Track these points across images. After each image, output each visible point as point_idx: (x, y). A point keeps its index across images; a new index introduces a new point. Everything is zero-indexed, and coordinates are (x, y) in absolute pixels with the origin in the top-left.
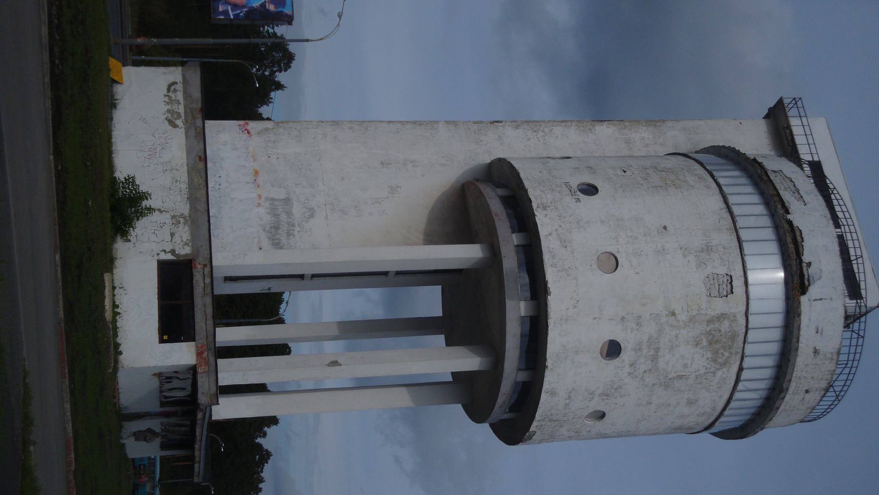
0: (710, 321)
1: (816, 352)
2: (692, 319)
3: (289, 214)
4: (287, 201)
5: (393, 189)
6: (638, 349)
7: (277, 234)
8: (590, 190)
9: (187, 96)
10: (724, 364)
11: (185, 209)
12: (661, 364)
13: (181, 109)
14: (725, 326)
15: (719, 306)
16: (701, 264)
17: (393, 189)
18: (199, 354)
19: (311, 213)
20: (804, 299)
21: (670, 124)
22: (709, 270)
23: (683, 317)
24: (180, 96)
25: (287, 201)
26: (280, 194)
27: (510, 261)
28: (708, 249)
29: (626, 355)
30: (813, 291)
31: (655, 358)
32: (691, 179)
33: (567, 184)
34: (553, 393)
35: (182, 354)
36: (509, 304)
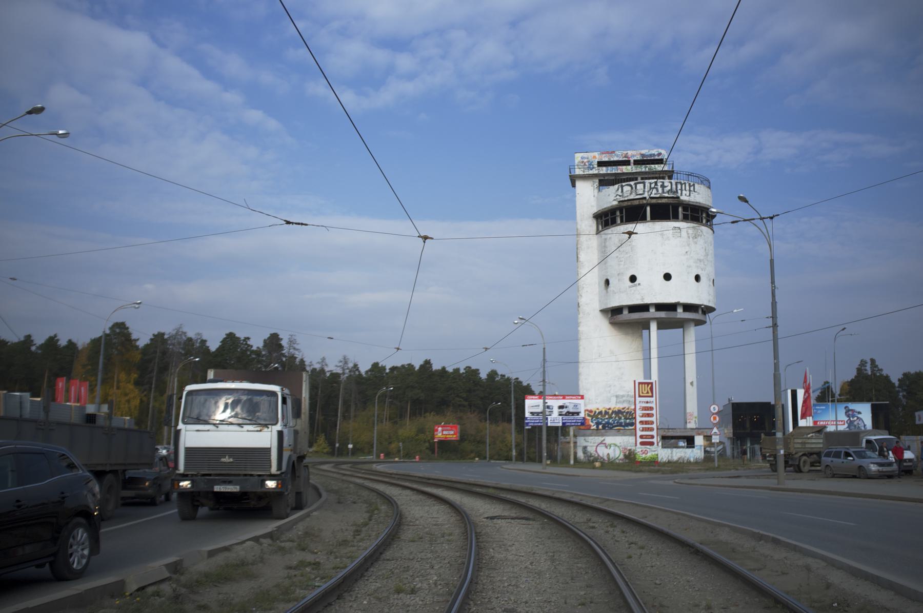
2: (689, 245)
3: (623, 396)
4: (617, 397)
6: (698, 267)
8: (633, 279)
12: (702, 258)
15: (684, 233)
16: (668, 239)
18: (699, 434)
21: (579, 227)
22: (671, 236)
23: (687, 249)
25: (617, 397)
26: (614, 400)
27: (662, 314)
31: (700, 261)
33: (630, 287)
36: (679, 316)
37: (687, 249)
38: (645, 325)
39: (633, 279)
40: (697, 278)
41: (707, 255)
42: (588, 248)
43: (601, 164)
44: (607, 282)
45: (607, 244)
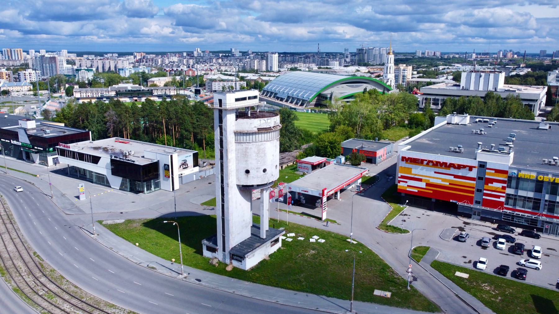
8: (265, 171)
19: (244, 220)
32: (262, 147)
43: (237, 100)
44: (247, 172)
45: (248, 151)
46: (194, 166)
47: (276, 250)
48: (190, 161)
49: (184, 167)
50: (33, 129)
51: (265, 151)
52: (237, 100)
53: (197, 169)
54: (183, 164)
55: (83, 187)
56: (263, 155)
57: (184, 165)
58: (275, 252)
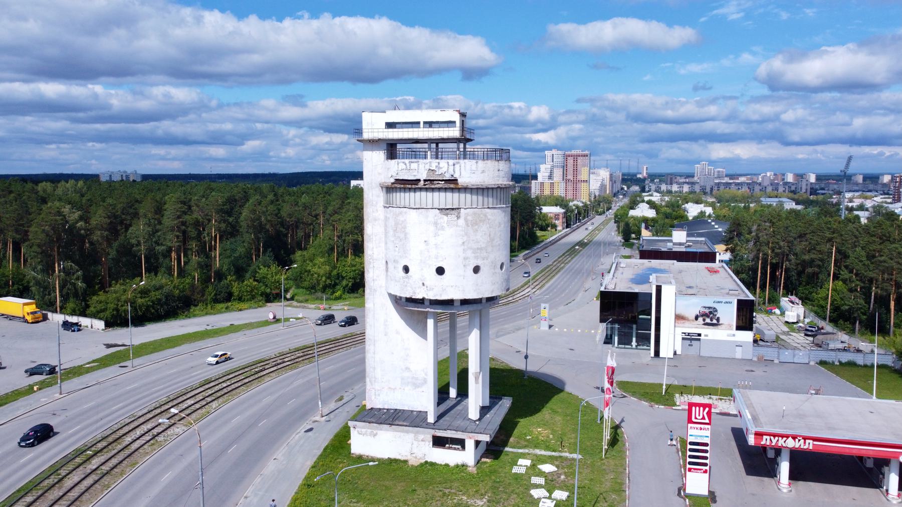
0: (468, 225)
1: (483, 172)
2: (466, 234)
4: (403, 379)
5: (398, 333)
6: (476, 258)
7: (416, 384)
8: (406, 269)
9: (363, 428)
10: (486, 216)
11: (411, 436)
12: (483, 246)
13: (369, 431)
14: (469, 218)
16: (443, 228)
17: (398, 333)
19: (407, 369)
20: (459, 181)
22: (445, 225)
23: (465, 238)
24: (364, 430)
28: (436, 224)
29: (479, 262)
30: (456, 176)
31: (481, 249)
32: (401, 218)
34: (492, 291)
35: (470, 444)
37: (465, 238)
38: (426, 315)
39: (406, 269)
40: (476, 270)
41: (492, 240)
42: (375, 220)
43: (390, 125)
46: (739, 328)
47: (452, 464)
48: (729, 314)
49: (708, 320)
50: (680, 244)
51: (405, 228)
52: (390, 125)
53: (747, 336)
54: (704, 315)
55: (547, 310)
56: (402, 236)
57: (710, 317)
58: (447, 465)
